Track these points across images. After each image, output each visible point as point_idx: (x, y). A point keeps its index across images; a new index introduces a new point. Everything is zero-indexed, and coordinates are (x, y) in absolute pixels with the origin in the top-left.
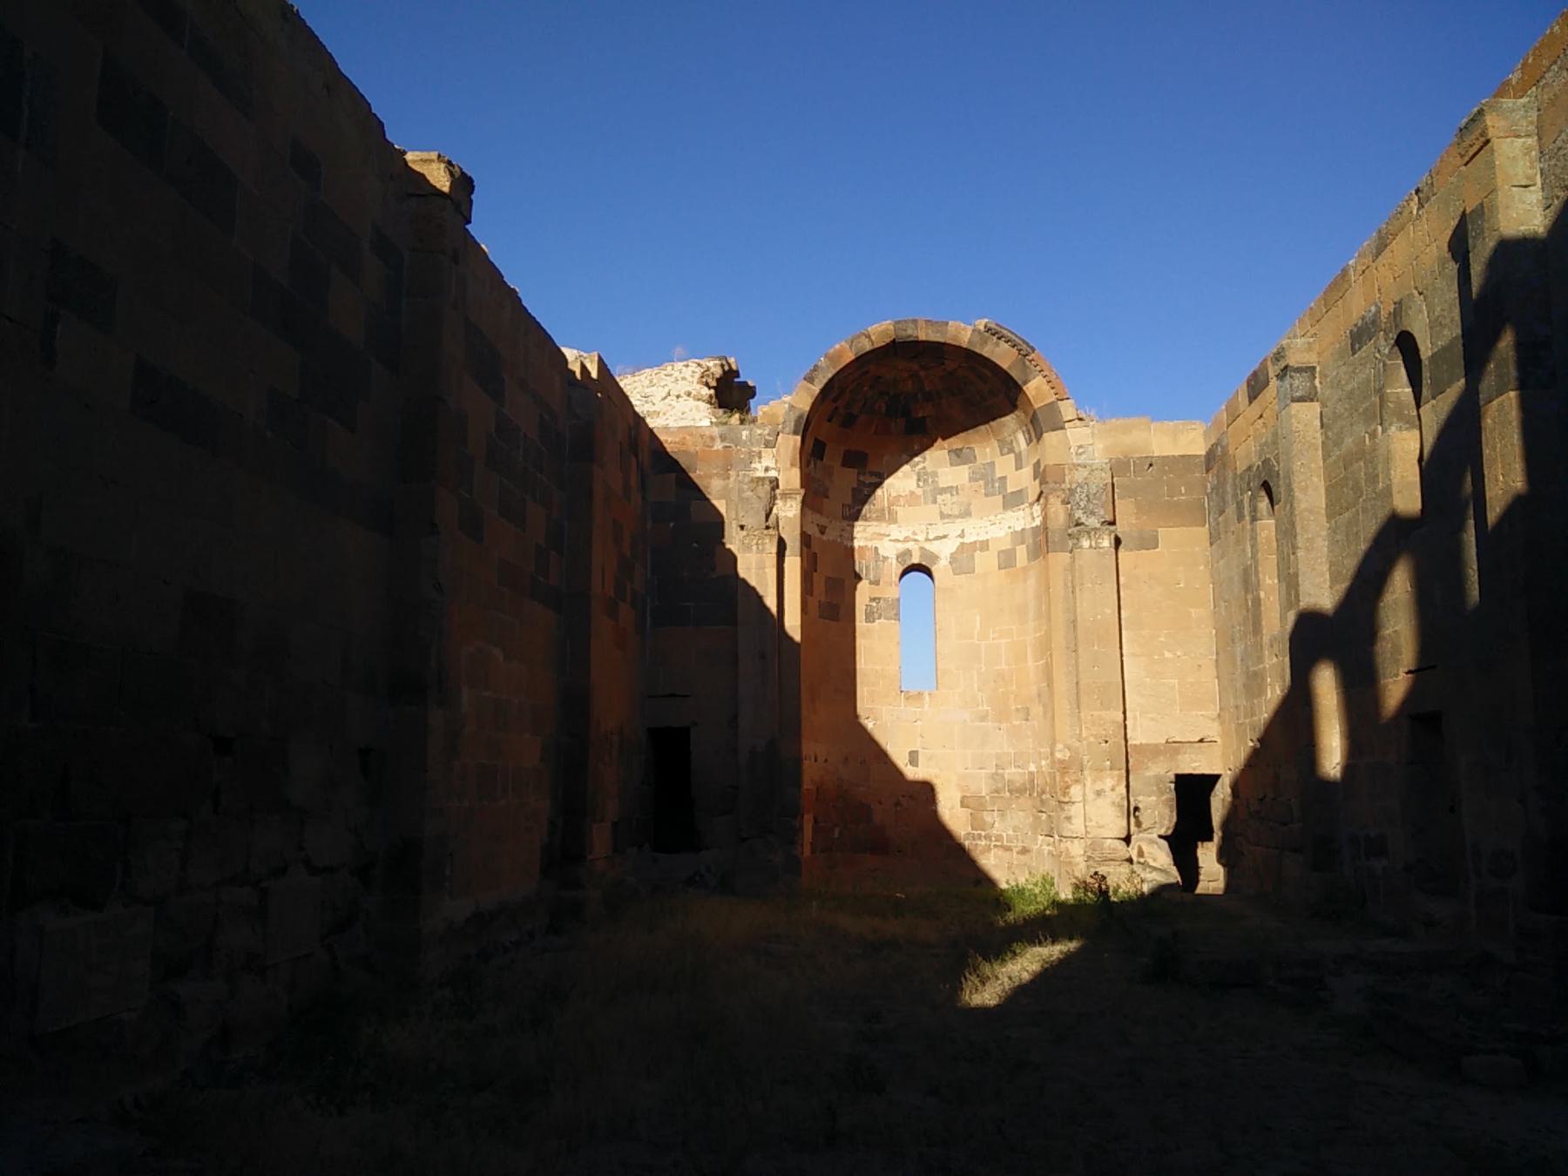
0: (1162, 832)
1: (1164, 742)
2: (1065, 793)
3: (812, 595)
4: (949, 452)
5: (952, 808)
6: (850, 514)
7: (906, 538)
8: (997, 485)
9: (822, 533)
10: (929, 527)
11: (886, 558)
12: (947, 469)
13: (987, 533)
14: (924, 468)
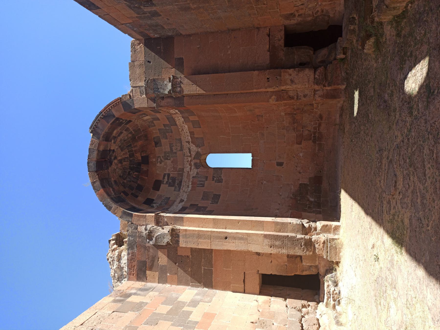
0: (312, 52)
1: (269, 52)
2: (292, 98)
3: (207, 207)
4: (156, 147)
5: (302, 148)
6: (178, 188)
7: (190, 165)
8: (167, 128)
9: (183, 201)
10: (185, 156)
11: (197, 173)
12: (163, 148)
13: (187, 132)
14: (163, 157)
